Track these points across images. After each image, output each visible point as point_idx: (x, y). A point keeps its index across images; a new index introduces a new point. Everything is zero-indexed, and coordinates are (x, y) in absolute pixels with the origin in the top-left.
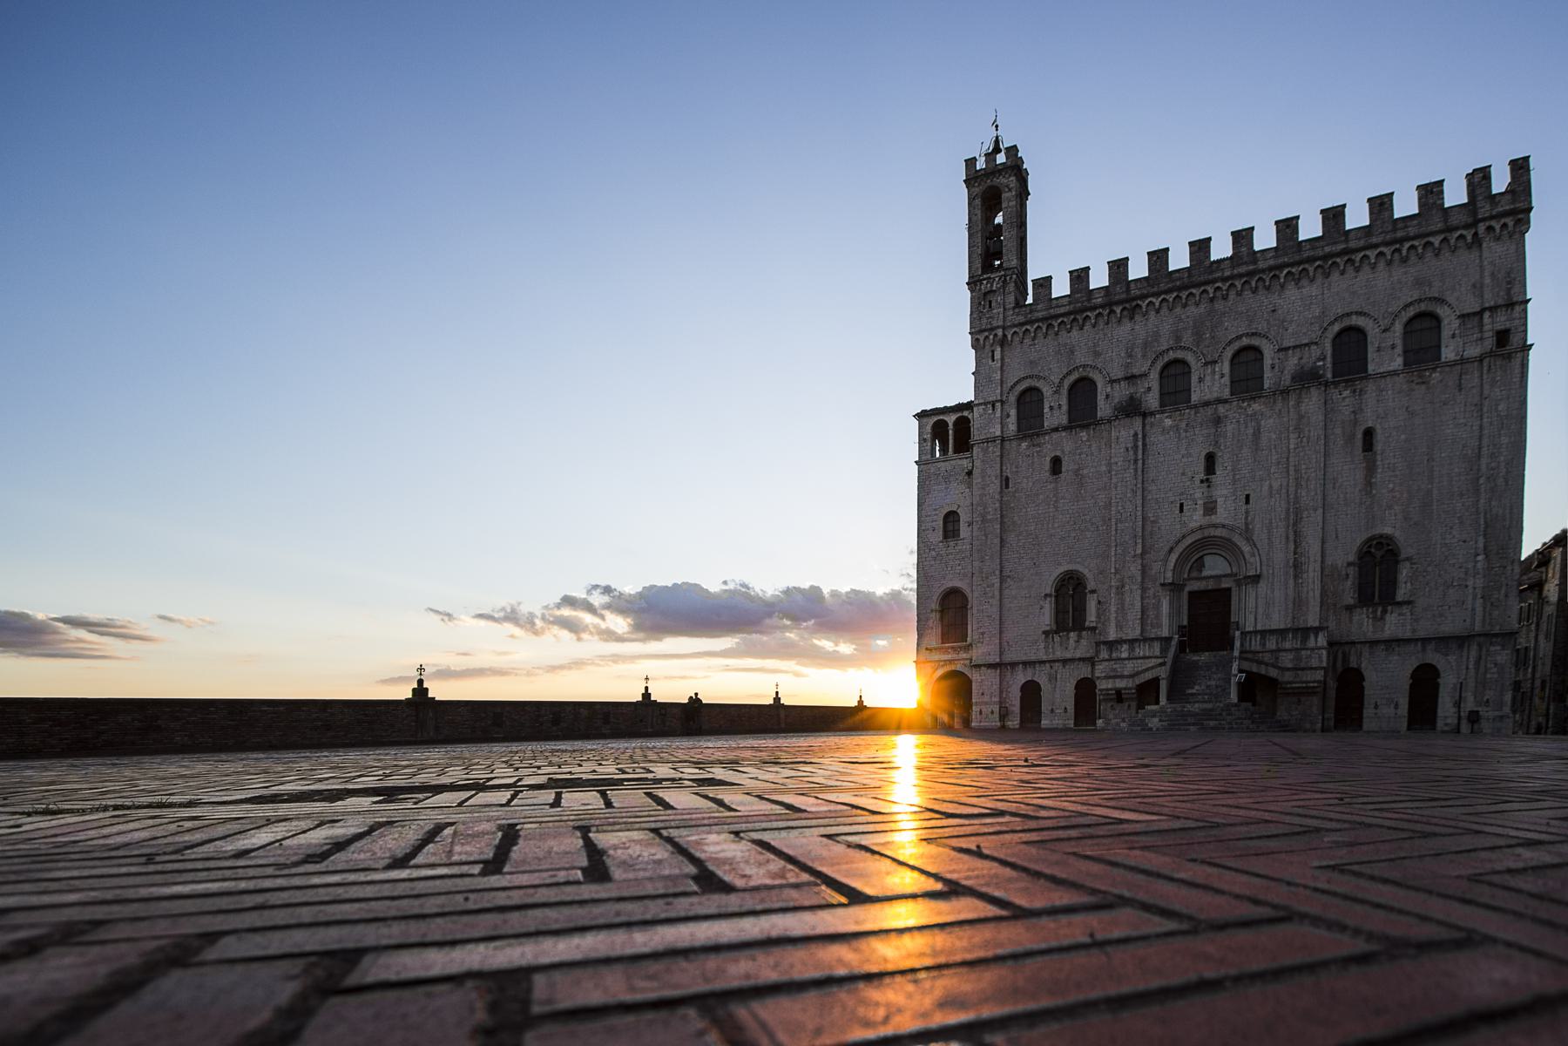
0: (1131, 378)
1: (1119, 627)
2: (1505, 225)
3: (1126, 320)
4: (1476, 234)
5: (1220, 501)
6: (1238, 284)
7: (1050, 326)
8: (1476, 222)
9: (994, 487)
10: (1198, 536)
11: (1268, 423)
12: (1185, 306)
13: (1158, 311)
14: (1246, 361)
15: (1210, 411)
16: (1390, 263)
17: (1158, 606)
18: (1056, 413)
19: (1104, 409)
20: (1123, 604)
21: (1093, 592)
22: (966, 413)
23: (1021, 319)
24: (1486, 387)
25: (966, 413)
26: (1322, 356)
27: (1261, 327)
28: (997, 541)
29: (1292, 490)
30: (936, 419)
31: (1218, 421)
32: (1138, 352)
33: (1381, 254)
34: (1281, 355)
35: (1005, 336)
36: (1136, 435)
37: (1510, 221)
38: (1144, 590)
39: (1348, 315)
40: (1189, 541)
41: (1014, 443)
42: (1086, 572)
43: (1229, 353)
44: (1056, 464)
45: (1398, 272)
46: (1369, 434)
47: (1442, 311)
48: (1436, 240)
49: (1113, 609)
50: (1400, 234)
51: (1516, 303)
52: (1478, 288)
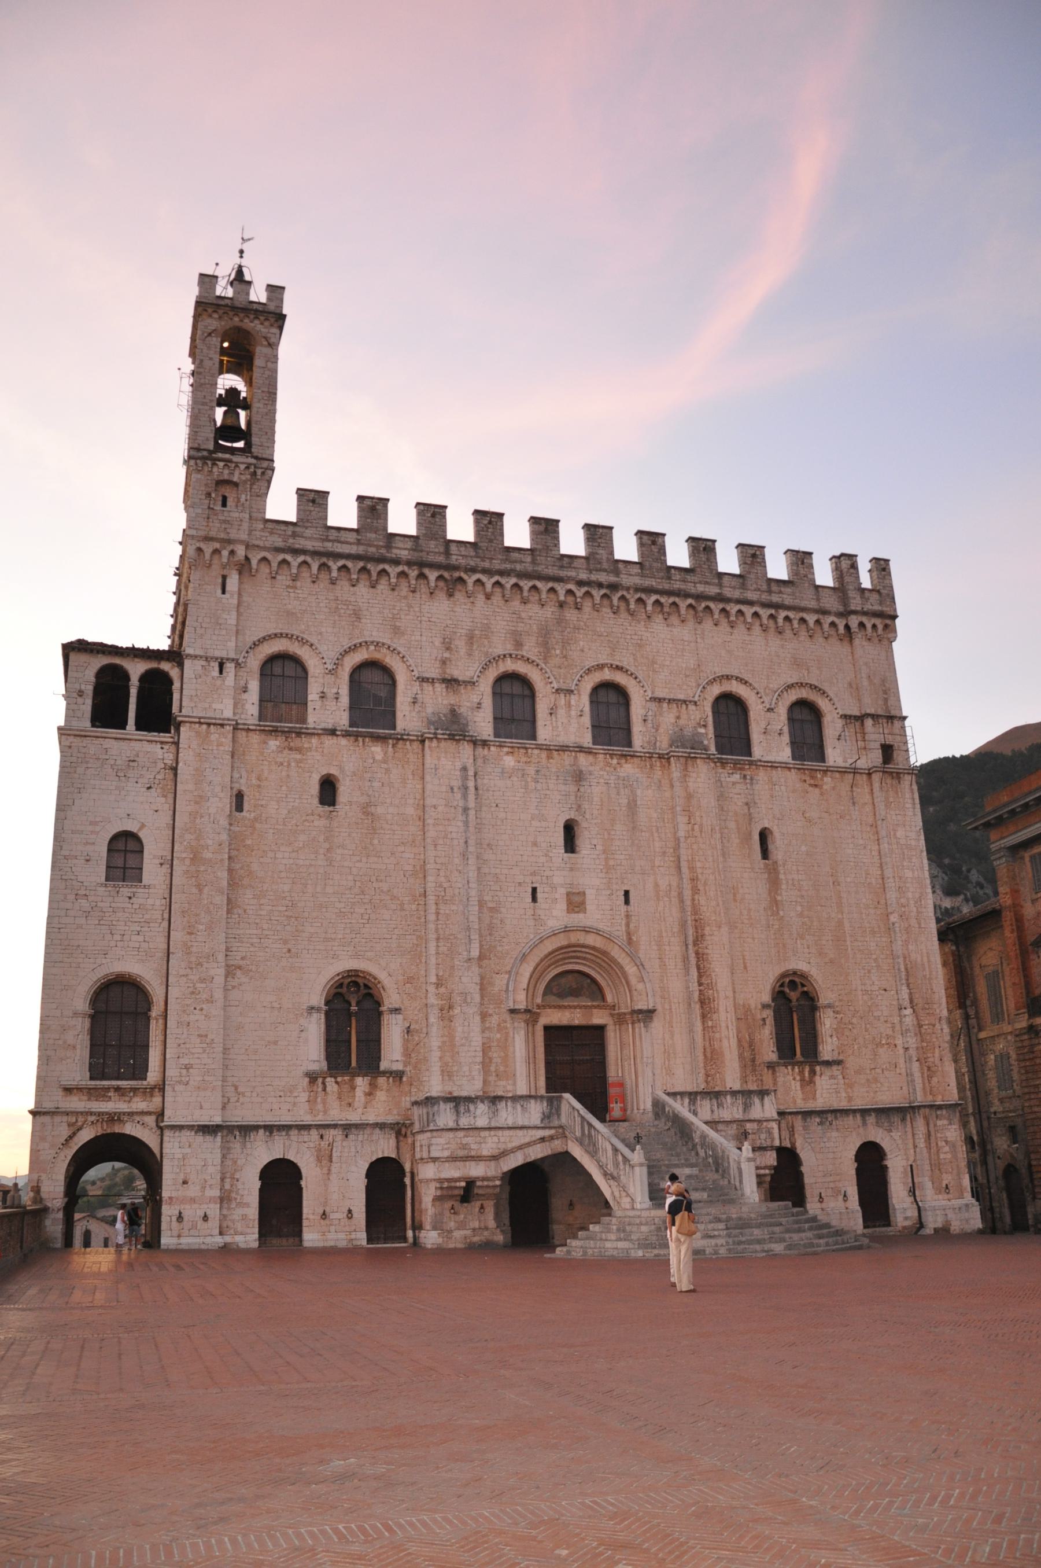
0: (451, 683)
1: (447, 1073)
2: (874, 626)
3: (441, 595)
4: (847, 627)
5: (590, 895)
6: (597, 594)
7: (323, 566)
8: (846, 614)
9: (220, 804)
10: (561, 941)
11: (646, 795)
12: (525, 602)
13: (488, 597)
14: (610, 702)
15: (567, 758)
16: (765, 629)
17: (505, 1045)
18: (331, 704)
19: (407, 718)
20: (451, 1037)
21: (397, 1011)
22: (165, 666)
23: (279, 543)
24: (881, 807)
25: (165, 666)
26: (700, 720)
28: (221, 900)
29: (687, 893)
30: (105, 660)
31: (579, 777)
32: (460, 644)
33: (756, 615)
34: (653, 705)
35: (247, 558)
36: (464, 769)
37: (878, 622)
38: (484, 1016)
39: (728, 677)
40: (549, 946)
41: (255, 738)
42: (382, 976)
43: (588, 685)
44: (328, 790)
46: (764, 836)
47: (823, 704)
48: (811, 619)
49: (435, 1042)
50: (775, 598)
51: (894, 718)
52: (854, 688)
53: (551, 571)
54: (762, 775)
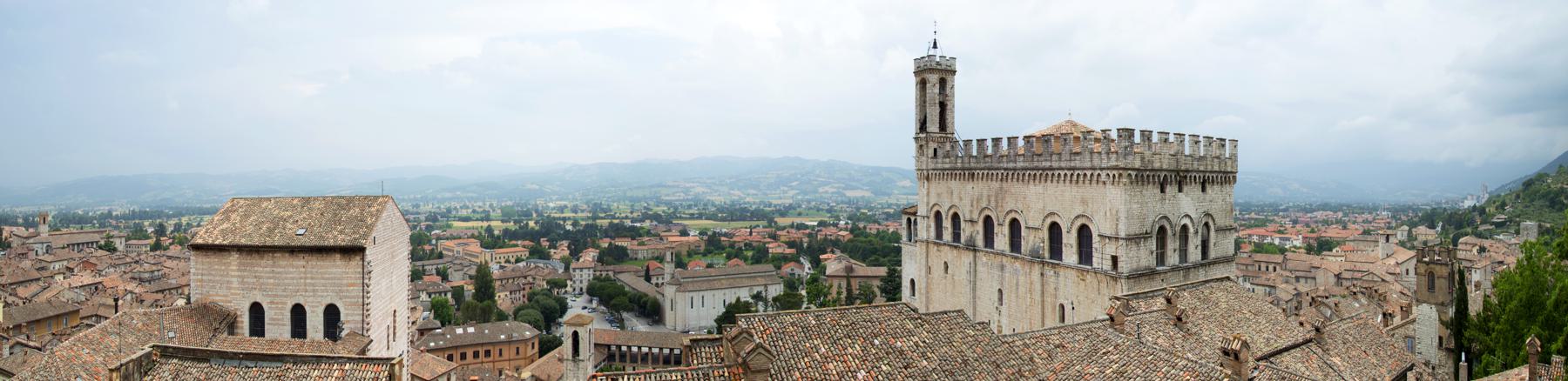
9: (923, 273)
11: (1022, 279)
19: (963, 240)
27: (1020, 206)
31: (1002, 267)
45: (1075, 188)
48: (1089, 173)
53: (996, 165)
54: (1062, 272)
